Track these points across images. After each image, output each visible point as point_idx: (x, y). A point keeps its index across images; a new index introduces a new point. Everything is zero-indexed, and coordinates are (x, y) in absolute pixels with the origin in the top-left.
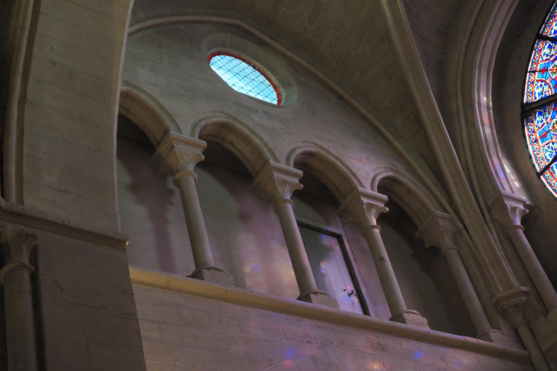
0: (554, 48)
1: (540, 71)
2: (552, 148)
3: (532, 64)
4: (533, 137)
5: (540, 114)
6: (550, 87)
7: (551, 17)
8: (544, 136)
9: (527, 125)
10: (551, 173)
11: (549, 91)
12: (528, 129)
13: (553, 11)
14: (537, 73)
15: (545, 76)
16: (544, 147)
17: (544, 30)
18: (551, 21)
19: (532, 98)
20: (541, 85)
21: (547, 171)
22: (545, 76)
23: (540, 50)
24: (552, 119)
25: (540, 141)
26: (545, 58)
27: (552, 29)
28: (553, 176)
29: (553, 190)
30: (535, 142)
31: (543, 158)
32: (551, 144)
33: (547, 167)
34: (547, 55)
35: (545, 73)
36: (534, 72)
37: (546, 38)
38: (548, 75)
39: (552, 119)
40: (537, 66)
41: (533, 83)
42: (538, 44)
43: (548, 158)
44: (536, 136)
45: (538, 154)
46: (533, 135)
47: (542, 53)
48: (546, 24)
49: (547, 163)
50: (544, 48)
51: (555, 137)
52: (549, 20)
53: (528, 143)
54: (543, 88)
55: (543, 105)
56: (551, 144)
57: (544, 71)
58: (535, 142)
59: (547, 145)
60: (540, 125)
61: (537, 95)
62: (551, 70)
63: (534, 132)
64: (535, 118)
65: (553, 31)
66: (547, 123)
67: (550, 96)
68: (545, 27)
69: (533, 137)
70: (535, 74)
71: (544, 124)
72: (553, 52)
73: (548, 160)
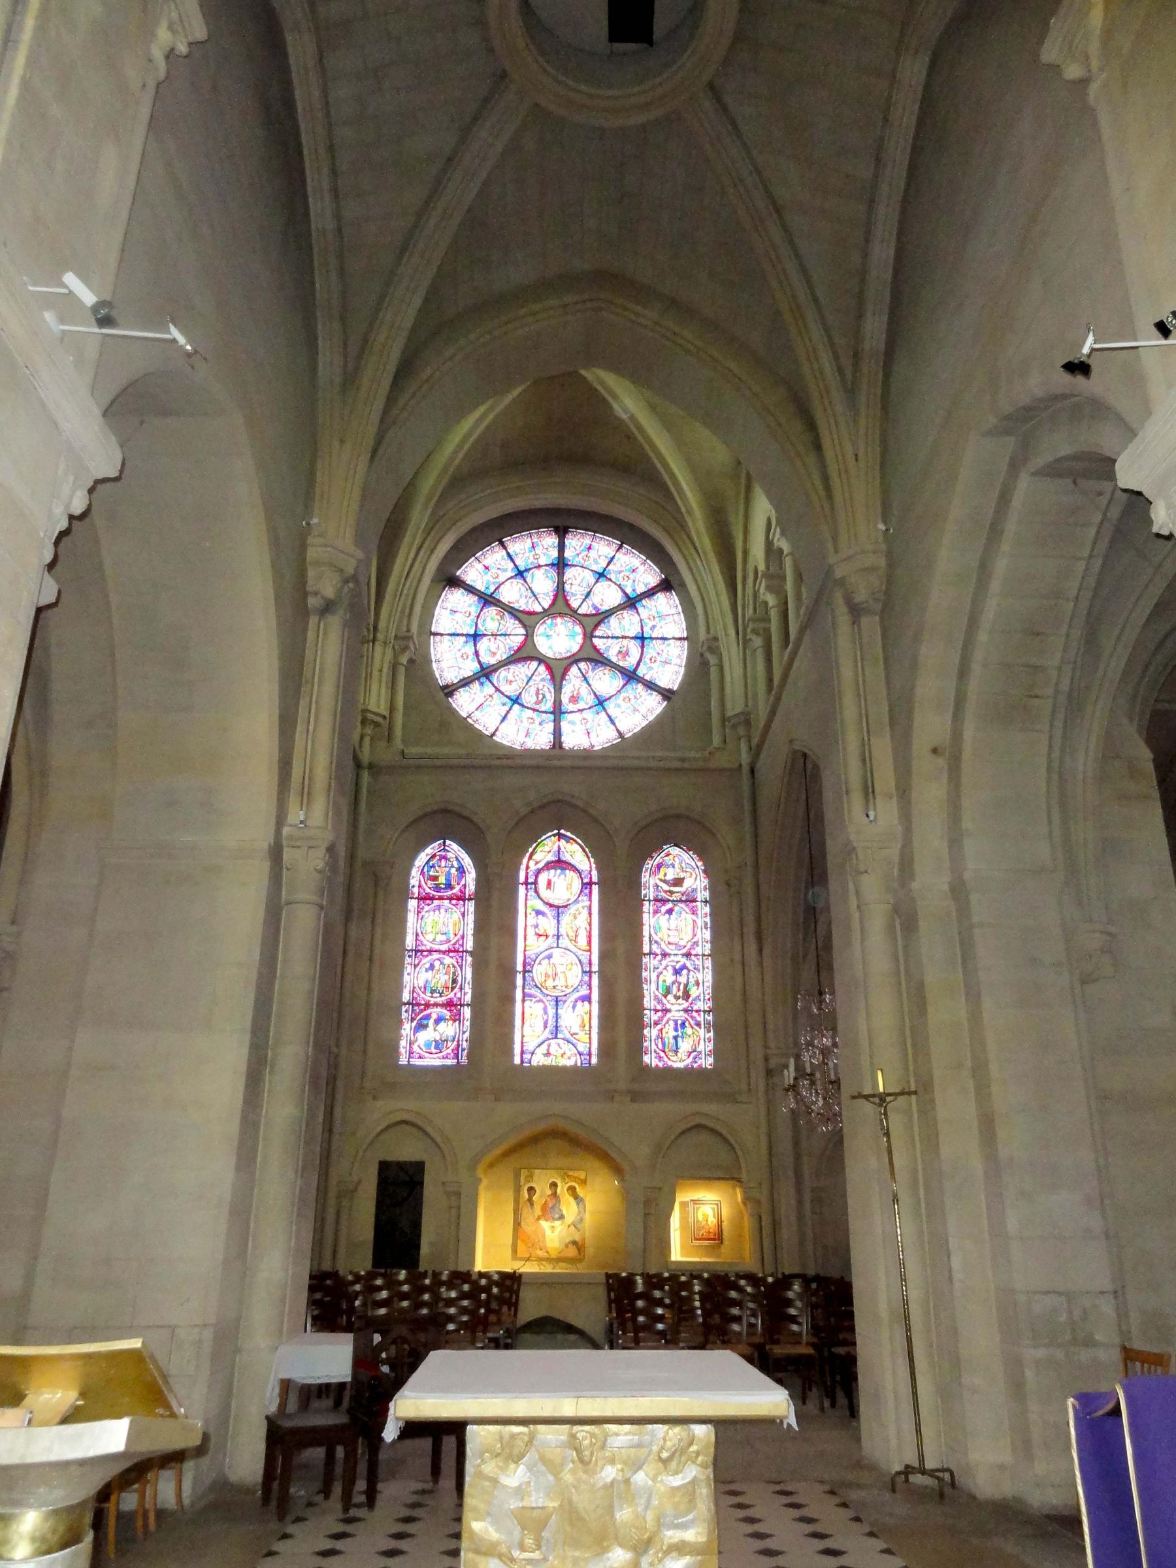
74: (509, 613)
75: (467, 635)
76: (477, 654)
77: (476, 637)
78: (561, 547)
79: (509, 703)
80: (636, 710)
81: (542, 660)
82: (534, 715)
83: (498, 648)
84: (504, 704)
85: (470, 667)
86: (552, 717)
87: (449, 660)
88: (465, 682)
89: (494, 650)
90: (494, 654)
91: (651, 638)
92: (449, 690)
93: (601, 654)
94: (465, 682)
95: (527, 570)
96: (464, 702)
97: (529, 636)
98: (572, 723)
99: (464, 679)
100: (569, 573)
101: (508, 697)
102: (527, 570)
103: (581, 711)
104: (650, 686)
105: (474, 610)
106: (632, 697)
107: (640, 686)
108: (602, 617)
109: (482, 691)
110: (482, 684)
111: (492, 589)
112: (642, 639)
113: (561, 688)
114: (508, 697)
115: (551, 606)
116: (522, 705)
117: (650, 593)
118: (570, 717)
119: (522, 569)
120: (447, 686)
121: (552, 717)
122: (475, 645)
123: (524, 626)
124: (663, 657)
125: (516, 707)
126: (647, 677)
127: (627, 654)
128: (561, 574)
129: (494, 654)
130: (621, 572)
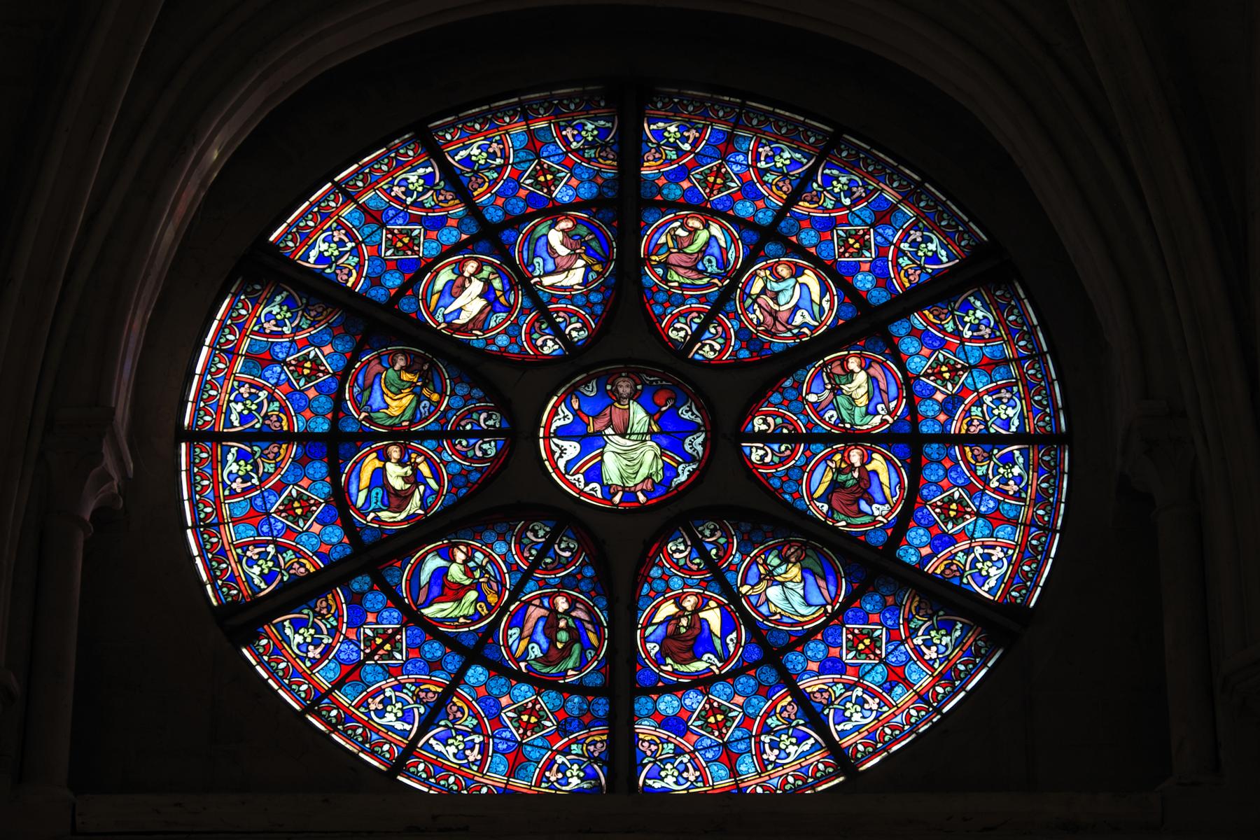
0: (438, 193)
1: (363, 208)
2: (260, 405)
3: (356, 172)
4: (231, 337)
5: (289, 303)
6: (360, 266)
7: (482, 118)
8: (261, 360)
9: (235, 295)
10: (213, 456)
11: (350, 274)
12: (231, 308)
13: (499, 109)
14: (352, 206)
15: (367, 230)
16: (241, 384)
17: (445, 128)
18: (477, 127)
19: (298, 249)
20: (341, 243)
21: (208, 445)
22: (367, 230)
23: (401, 165)
24: (308, 342)
25: (240, 362)
26: (397, 191)
27: (465, 147)
28: (215, 469)
29: (191, 499)
30: (227, 352)
31: (219, 407)
32: (263, 395)
33: (217, 438)
34: (408, 193)
35: (375, 227)
36: (350, 198)
37: (435, 153)
38: (376, 238)
39: (308, 342)
40: (366, 189)
41: (326, 217)
42: (405, 143)
43: (234, 418)
44: (240, 341)
45: (214, 387)
46: (232, 332)
47: (400, 175)
48: (460, 120)
49: (221, 427)
50: (414, 169)
51: (286, 387)
52: (474, 118)
53: (208, 341)
54: (342, 254)
55: (315, 291)
56: (263, 395)
57: (373, 217)
58: (227, 352)
59: (252, 386)
60: (270, 327)
61: (313, 254)
62: (391, 231)
63: (241, 327)
64: (270, 301)
65: (463, 153)
66: (292, 341)
67: (342, 287)
68: (453, 125)
69: (231, 337)
70: (345, 204)
71: (282, 334)
72: (428, 199)
73: (229, 423)
74: (451, 361)
75: (305, 438)
76: (340, 499)
77: (335, 447)
78: (629, 149)
79: (453, 662)
80: (896, 677)
81: (566, 514)
82: (548, 701)
83: (416, 479)
84: (434, 665)
85: (320, 538)
86: (601, 707)
87: (242, 522)
88: (297, 595)
89: (398, 484)
90: (404, 497)
91: (946, 439)
92: (250, 617)
93: (774, 495)
94: (297, 595)
95: (514, 222)
96: (300, 658)
97: (520, 435)
98: (676, 724)
99: (296, 581)
100: (662, 233)
101: (451, 642)
102: (514, 222)
103: (703, 682)
104: (946, 599)
105: (327, 356)
106: (880, 632)
107: (909, 602)
108: (774, 366)
109: (357, 621)
110: (355, 601)
111: (393, 281)
112: (906, 441)
113: (634, 610)
114: (451, 642)
115: (594, 339)
116: (497, 668)
117: (940, 291)
118: (668, 705)
119: (494, 215)
120: (231, 609)
121: (601, 707)
122: (335, 473)
123: (502, 404)
124: (987, 506)
125: (476, 674)
126: (935, 567)
127: (865, 487)
128: (630, 232)
129: (397, 499)
130: (831, 224)
